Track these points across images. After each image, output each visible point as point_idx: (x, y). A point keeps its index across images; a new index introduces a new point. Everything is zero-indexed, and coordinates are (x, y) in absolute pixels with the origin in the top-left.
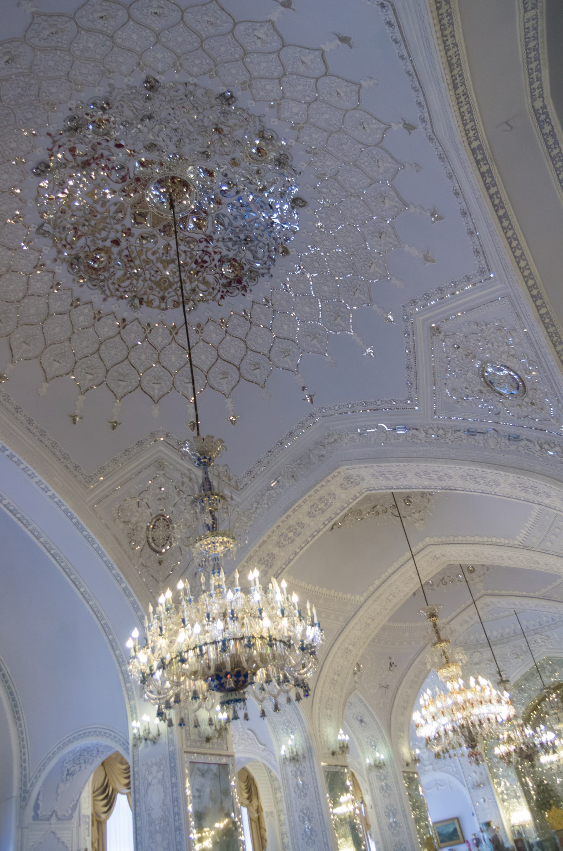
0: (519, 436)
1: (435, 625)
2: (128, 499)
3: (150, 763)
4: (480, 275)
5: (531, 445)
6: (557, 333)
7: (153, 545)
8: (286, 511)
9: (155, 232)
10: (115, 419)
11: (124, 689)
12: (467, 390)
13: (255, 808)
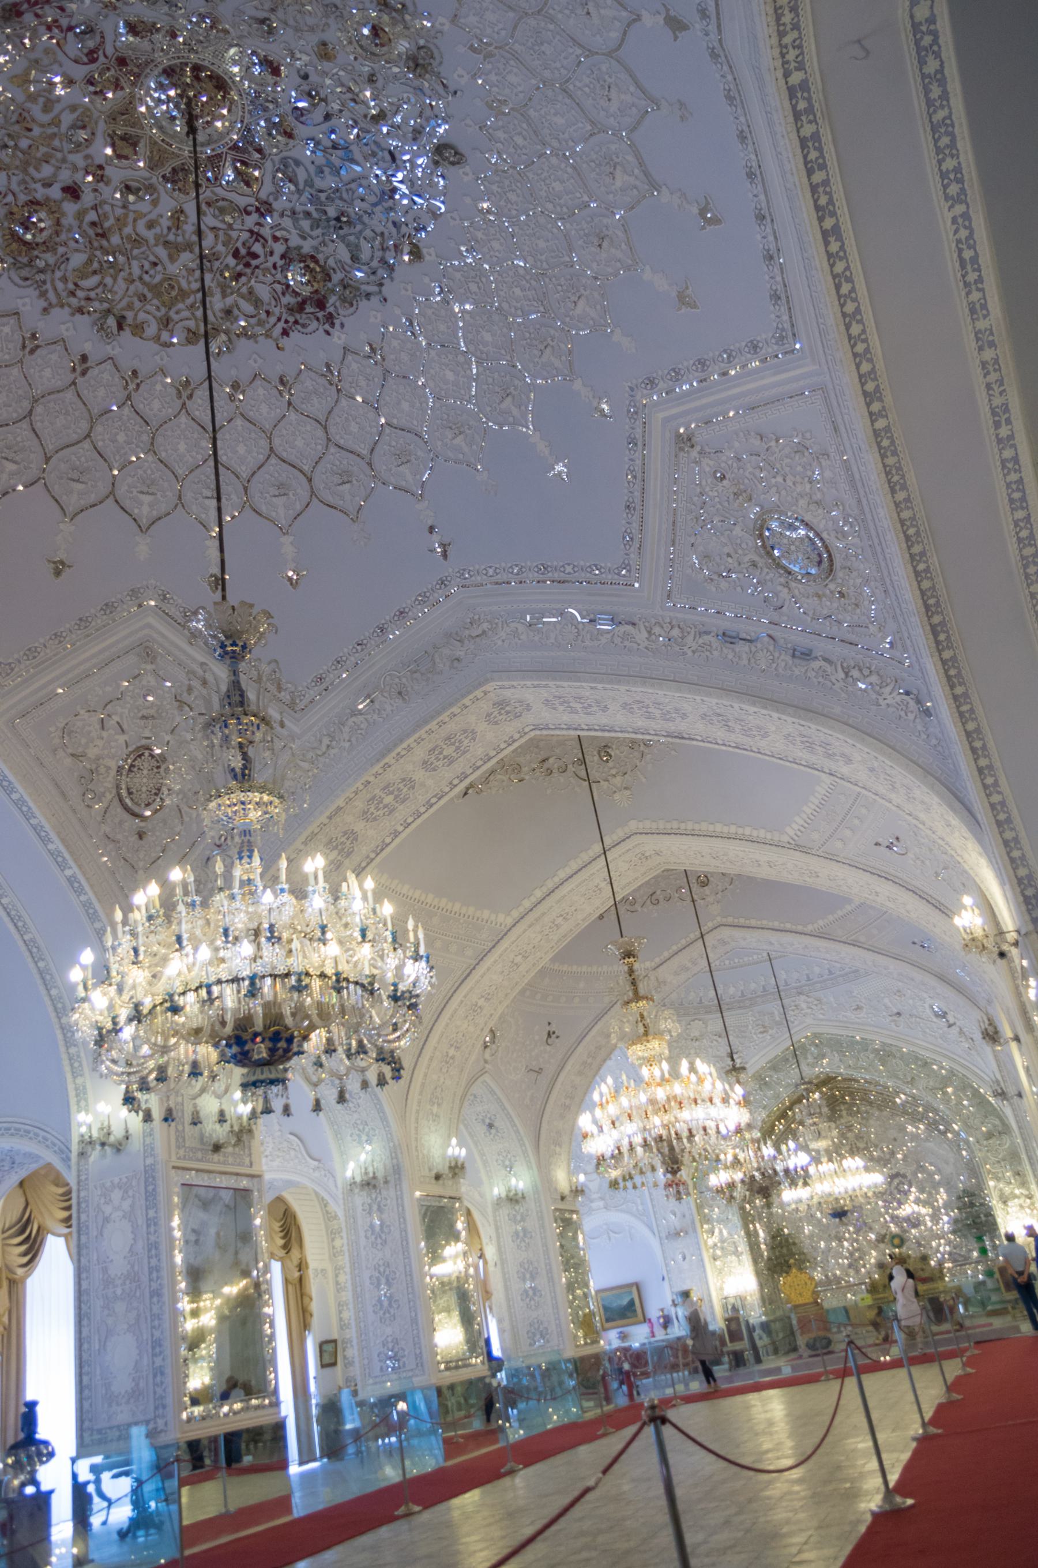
1: (631, 971)
2: (82, 712)
3: (109, 1184)
4: (777, 343)
5: (829, 669)
6: (899, 469)
7: (128, 801)
8: (383, 756)
9: (154, 180)
10: (61, 555)
11: (64, 1056)
12: (730, 560)
13: (296, 1262)
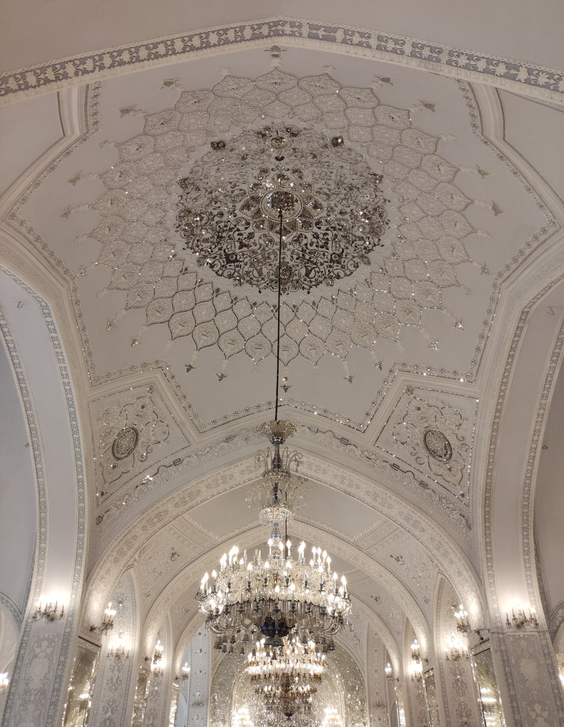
0: (427, 485)
3: (42, 637)
5: (433, 495)
